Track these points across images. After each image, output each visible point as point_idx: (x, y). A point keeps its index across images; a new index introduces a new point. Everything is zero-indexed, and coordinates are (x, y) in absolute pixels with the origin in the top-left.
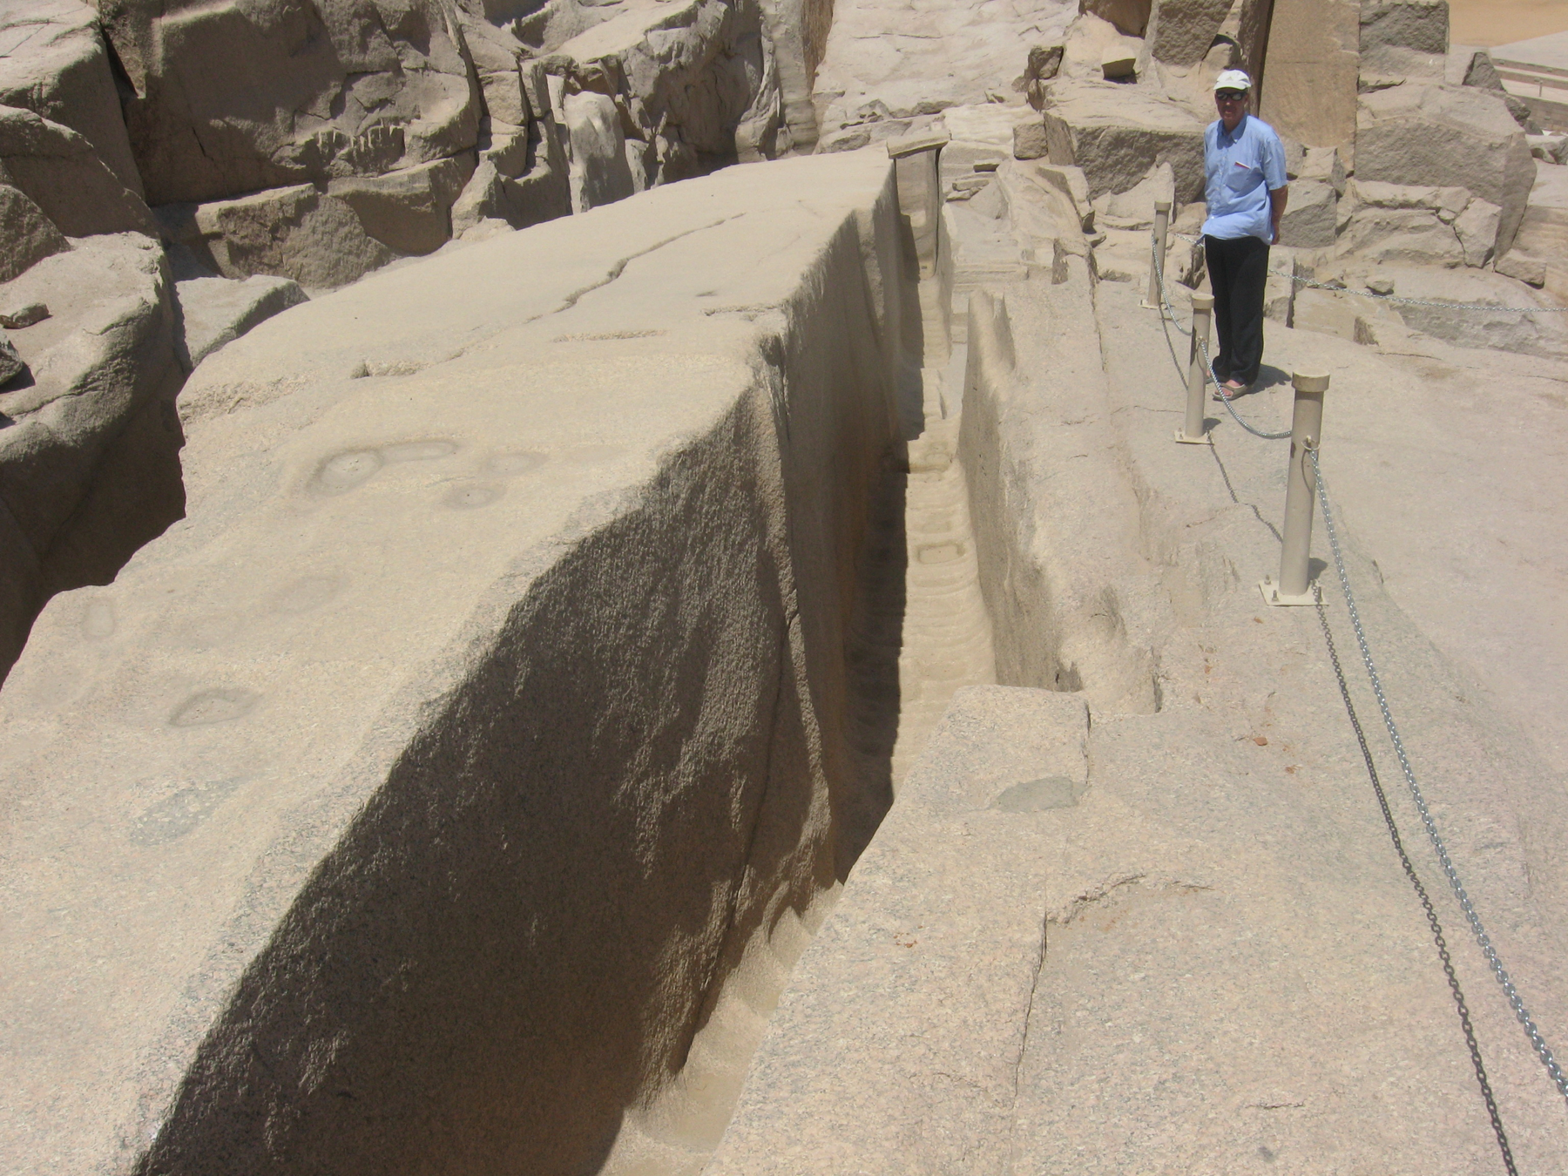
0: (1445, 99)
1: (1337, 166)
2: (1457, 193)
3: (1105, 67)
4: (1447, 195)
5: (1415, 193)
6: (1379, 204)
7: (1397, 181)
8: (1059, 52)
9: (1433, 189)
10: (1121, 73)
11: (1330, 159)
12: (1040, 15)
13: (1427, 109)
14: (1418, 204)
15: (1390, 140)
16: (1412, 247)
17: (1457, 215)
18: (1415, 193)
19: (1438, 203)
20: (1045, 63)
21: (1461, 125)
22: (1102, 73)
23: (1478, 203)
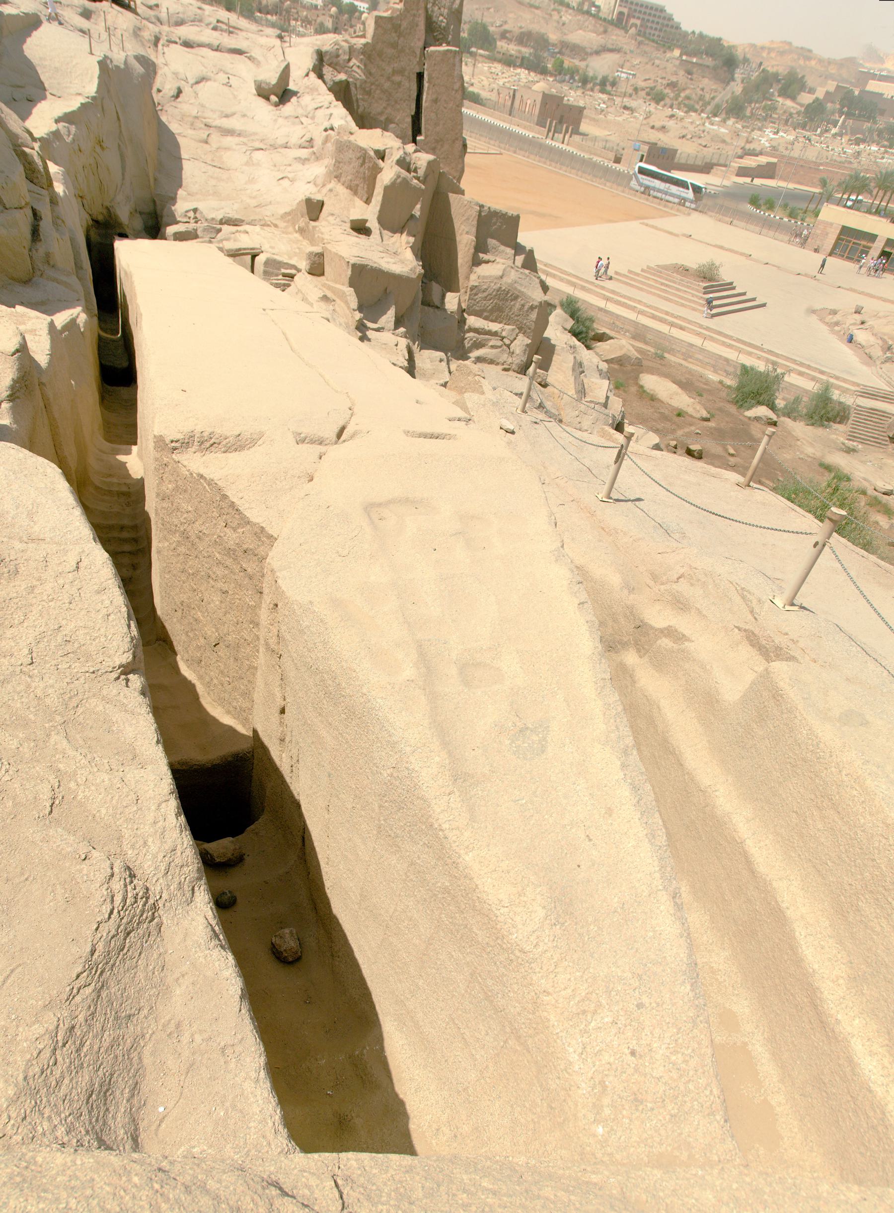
0: (513, 275)
1: (459, 304)
2: (513, 330)
3: (352, 222)
4: (506, 329)
5: (494, 327)
6: (476, 331)
7: (486, 318)
8: (322, 204)
9: (501, 325)
10: (360, 228)
11: (456, 300)
12: (289, 169)
13: (504, 279)
14: (495, 334)
15: (485, 294)
16: (490, 357)
17: (512, 342)
18: (494, 327)
19: (504, 334)
20: (314, 209)
21: (520, 291)
22: (349, 225)
23: (521, 336)
